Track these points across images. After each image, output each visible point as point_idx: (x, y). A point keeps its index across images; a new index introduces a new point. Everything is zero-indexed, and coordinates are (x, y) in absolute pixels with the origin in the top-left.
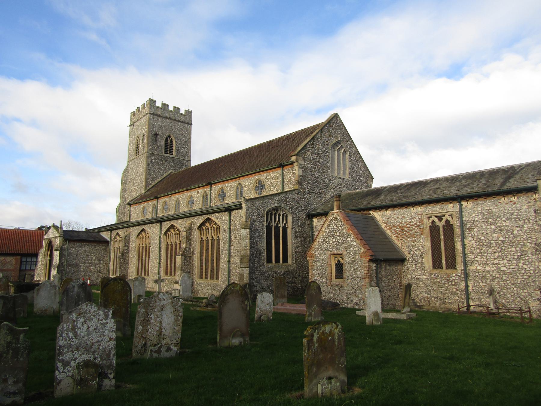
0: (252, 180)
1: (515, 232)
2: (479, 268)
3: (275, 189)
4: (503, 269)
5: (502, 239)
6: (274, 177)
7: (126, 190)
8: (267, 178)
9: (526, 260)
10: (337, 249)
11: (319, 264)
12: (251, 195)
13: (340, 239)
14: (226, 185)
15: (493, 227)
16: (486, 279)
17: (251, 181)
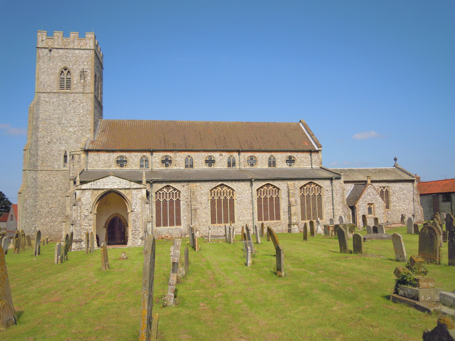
0: (284, 155)
1: (408, 195)
2: (397, 208)
3: (305, 164)
4: (405, 208)
5: (404, 197)
6: (303, 157)
8: (298, 156)
9: (411, 205)
10: (371, 201)
11: (362, 208)
12: (284, 165)
13: (373, 197)
14: (258, 155)
15: (402, 193)
16: (400, 212)
17: (284, 156)
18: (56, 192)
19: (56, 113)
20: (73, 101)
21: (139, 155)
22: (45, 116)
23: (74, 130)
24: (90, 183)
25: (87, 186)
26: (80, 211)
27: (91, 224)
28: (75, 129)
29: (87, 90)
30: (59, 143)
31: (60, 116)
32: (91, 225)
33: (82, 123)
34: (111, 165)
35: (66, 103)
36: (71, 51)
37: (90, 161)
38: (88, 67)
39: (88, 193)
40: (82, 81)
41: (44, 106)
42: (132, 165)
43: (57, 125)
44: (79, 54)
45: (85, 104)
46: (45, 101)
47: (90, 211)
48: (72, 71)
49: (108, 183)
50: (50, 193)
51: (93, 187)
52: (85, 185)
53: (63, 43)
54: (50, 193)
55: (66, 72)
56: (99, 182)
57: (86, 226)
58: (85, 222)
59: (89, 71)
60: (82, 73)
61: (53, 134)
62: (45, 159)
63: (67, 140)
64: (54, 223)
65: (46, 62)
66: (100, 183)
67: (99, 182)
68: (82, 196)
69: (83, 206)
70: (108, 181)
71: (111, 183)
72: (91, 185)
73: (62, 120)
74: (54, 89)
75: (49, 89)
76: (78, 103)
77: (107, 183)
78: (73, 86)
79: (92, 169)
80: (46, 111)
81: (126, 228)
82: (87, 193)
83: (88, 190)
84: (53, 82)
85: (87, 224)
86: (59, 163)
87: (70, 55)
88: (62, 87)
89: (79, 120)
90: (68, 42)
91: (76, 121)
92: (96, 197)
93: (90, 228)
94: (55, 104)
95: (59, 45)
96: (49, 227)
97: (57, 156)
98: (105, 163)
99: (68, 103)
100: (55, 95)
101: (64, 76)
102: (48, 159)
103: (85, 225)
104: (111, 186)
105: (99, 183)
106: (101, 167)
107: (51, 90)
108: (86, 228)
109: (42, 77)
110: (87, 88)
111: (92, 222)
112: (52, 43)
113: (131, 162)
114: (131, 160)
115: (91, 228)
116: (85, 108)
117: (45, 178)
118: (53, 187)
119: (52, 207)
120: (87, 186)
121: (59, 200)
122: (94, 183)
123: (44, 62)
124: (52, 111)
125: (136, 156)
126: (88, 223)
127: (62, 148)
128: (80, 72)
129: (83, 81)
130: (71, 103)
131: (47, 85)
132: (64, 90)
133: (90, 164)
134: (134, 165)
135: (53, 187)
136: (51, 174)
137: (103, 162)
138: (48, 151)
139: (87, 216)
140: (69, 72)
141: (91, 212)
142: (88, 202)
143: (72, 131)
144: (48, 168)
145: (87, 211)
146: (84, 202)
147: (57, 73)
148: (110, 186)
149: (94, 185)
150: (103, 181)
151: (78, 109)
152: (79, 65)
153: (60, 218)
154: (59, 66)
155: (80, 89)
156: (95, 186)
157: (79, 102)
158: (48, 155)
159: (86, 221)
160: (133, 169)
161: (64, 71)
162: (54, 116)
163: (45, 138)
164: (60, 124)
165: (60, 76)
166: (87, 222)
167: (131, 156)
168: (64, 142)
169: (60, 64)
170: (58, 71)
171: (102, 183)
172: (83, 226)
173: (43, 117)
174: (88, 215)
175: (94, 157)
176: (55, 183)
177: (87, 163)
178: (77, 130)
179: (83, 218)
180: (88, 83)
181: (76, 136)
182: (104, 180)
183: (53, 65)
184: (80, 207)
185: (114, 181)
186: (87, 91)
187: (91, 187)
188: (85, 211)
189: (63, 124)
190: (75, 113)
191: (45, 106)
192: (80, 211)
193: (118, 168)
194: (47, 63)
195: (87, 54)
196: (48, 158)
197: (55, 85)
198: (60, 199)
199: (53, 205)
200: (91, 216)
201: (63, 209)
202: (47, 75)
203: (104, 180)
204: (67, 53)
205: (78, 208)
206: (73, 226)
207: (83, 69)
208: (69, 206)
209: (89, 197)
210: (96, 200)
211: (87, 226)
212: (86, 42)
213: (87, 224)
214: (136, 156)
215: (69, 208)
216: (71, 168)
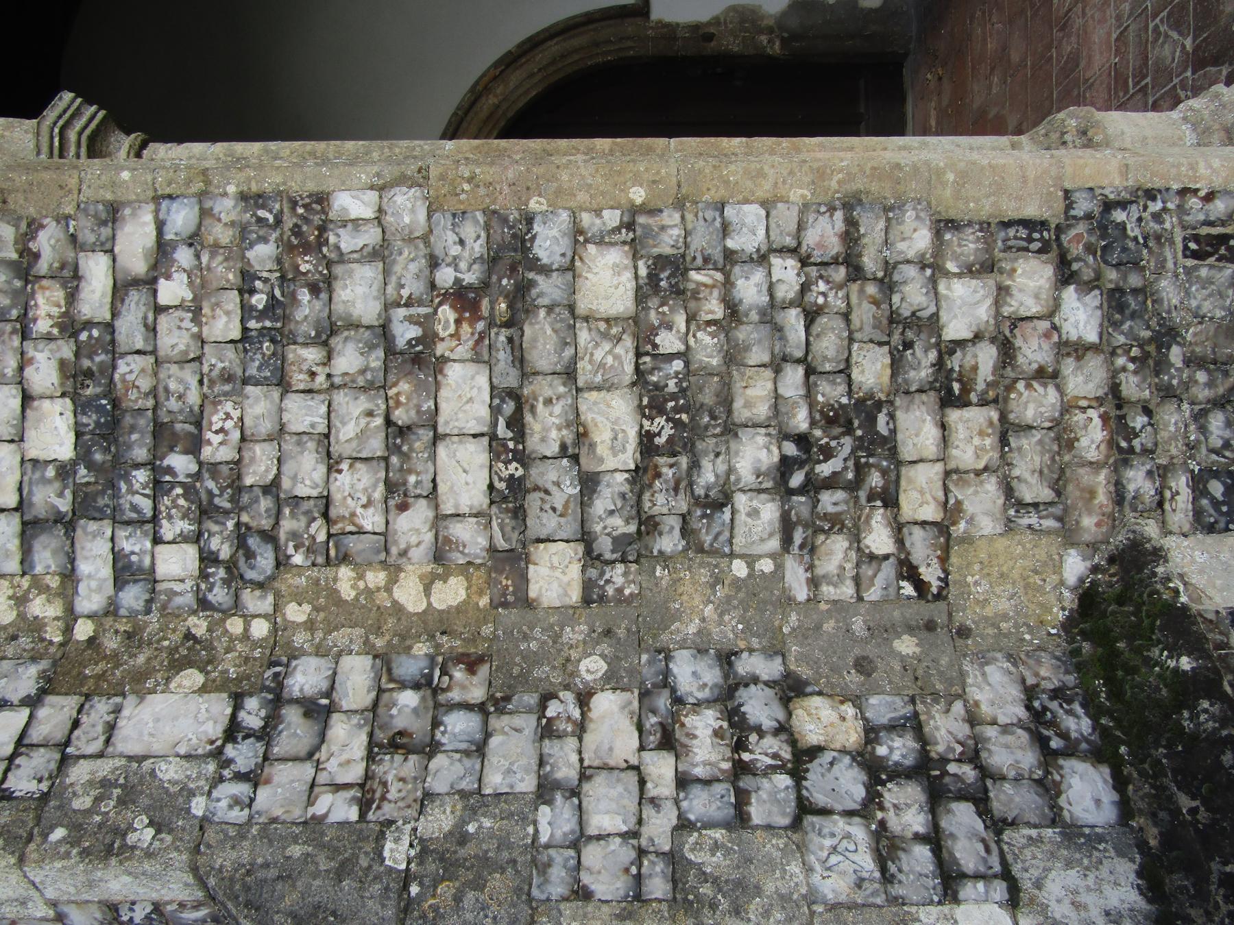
81: (669, 31)
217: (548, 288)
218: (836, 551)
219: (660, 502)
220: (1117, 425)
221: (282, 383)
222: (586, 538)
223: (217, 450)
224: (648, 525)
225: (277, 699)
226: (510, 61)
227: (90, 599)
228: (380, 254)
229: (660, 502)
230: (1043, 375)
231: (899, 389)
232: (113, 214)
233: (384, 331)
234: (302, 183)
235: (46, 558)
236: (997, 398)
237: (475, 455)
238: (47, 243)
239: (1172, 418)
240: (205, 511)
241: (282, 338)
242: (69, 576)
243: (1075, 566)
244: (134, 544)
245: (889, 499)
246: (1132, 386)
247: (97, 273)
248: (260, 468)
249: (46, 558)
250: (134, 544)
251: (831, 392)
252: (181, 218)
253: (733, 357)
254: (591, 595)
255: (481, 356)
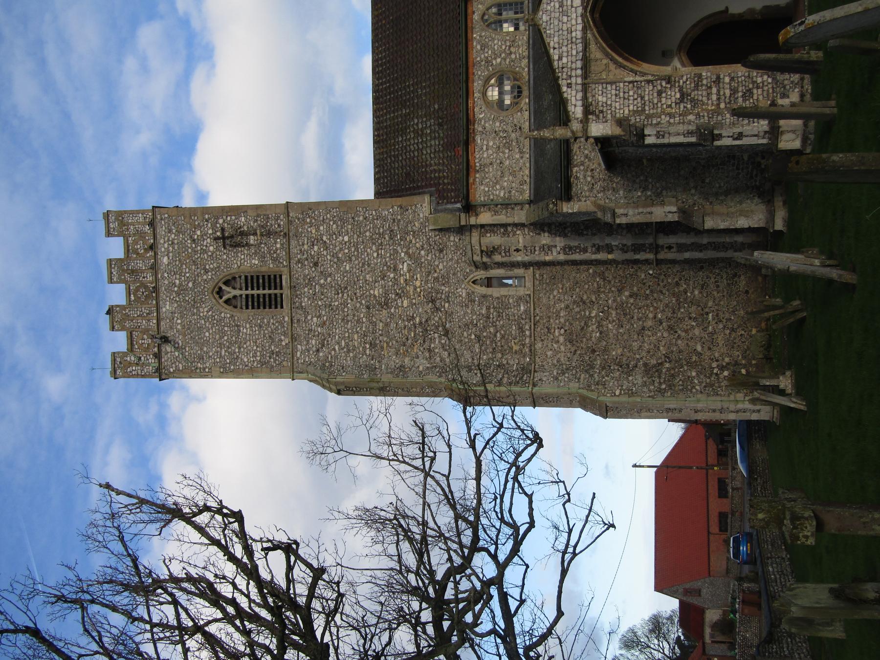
7: (402, 367)
18: (606, 308)
19: (354, 315)
20: (316, 264)
21: (481, 36)
22: (365, 348)
23: (406, 258)
24: (564, 89)
25: (573, 99)
26: (663, 117)
27: (714, 78)
28: (403, 254)
29: (279, 225)
30: (449, 302)
31: (363, 302)
32: (718, 78)
33: (382, 235)
34: (515, 125)
35: (321, 286)
36: (163, 278)
37: (502, 195)
38: (209, 225)
39: (601, 97)
40: (252, 240)
41: (333, 353)
42: (513, 56)
43: (392, 310)
44: (171, 254)
45: (321, 228)
46: (318, 351)
47: (664, 84)
48: (225, 273)
49: (565, 28)
50: (610, 326)
51: (579, 80)
52: (571, 108)
53: (142, 303)
54: (610, 326)
55: (229, 293)
56: (560, 58)
57: (722, 93)
58: (705, 99)
59: (221, 221)
60: (228, 242)
61: (421, 323)
62: (499, 344)
63: (436, 279)
64: (707, 310)
65: (201, 349)
66: (565, 54)
67: (560, 58)
68: (609, 116)
69: (647, 108)
70: (556, 29)
71: (565, 19)
72: (569, 86)
73: (375, 296)
74: (281, 323)
75: (283, 338)
76: (319, 249)
77: (565, 33)
78: (270, 266)
79: (526, 187)
80: (347, 345)
81: (733, 15)
82: (600, 98)
83: (589, 95)
84: (261, 326)
85: (714, 90)
86: (511, 301)
87: (177, 282)
88: (275, 302)
89: (374, 244)
90: (137, 290)
91: (375, 255)
92: (612, 67)
93: (727, 80)
94: (325, 318)
95: (148, 314)
96: (721, 326)
97: (488, 308)
98: (508, 145)
99: (322, 281)
100: (298, 321)
101: (241, 296)
102: (498, 335)
103: (714, 97)
104: (574, 16)
105: (565, 60)
106: (522, 157)
107: (285, 334)
108: (728, 92)
109: (246, 360)
110: (272, 225)
111: (704, 74)
112: (145, 337)
113: (505, 59)
114: (499, 60)
115: (729, 75)
116: (334, 226)
117: (558, 342)
118: (590, 318)
119: (655, 317)
120: (573, 99)
121: (631, 296)
122: (565, 76)
123: (201, 358)
124: (349, 326)
125: (484, 47)
126: (710, 88)
127: (464, 295)
128: (225, 248)
129: (252, 237)
130: (322, 272)
131: (270, 346)
132: (282, 295)
133: (510, 192)
134: (513, 49)
135: (590, 318)
136: (546, 325)
137: (504, 153)
138: (473, 337)
139: (683, 95)
140: (227, 283)
141: (668, 82)
142: (631, 93)
143: (408, 265)
144: (527, 333)
145: (664, 95)
146: (631, 108)
147: (232, 316)
148: (574, 22)
149: (570, 77)
150: (557, 46)
151: (341, 249)
152: (205, 252)
153: (692, 293)
154: (210, 313)
155: (278, 246)
156: (573, 74)
157: (316, 248)
158: (485, 334)
159: (700, 94)
160: (526, 54)
161: (225, 298)
162: (364, 320)
163: (432, 346)
164: (386, 304)
165: (241, 308)
166: (705, 93)
167: (483, 63)
168: (443, 288)
169: (206, 309)
170: (227, 313)
171: (564, 49)
172: (718, 105)
173: (368, 352)
174: (681, 91)
175: (488, 180)
176: (577, 309)
177: (508, 205)
178: (405, 250)
179: (689, 106)
180: (256, 221)
181: (423, 253)
182: (552, 44)
183: (208, 331)
184: (649, 117)
185: (557, 5)
186: (282, 223)
187: (579, 87)
188: (664, 100)
189: (386, 293)
190: (353, 258)
191: (334, 349)
192: (663, 117)
193: (523, 103)
194: (205, 349)
195: (170, 231)
196: (495, 336)
197: (269, 322)
198: (627, 293)
199: (647, 317)
200: (685, 78)
201: (662, 284)
202: (239, 348)
203: (552, 42)
204: (169, 290)
205: (654, 122)
206: (720, 137)
207: (216, 239)
208: (649, 210)
209: (614, 92)
210: (624, 67)
211: (718, 91)
212: (134, 235)
213: (714, 90)
214: (484, 47)
215: (653, 209)
216: (526, 259)
217: (722, 80)
218: (748, 102)
219: (732, 99)
220: (773, 90)
221: (698, 90)
222: (725, 102)
223: (692, 96)
224: (731, 101)
225: (700, 116)
226: (694, 26)
227: (681, 110)
228: (706, 78)
229: (732, 99)
230: (767, 86)
231: (753, 88)
232: (682, 76)
233: (707, 85)
234: (699, 72)
235: (678, 106)
236: (762, 88)
237: (715, 96)
238: (677, 79)
239: (778, 89)
240: (691, 102)
241: (698, 86)
242: (680, 108)
243: (769, 102)
244: (685, 105)
245: (752, 97)
246: (775, 86)
247: (681, 82)
248: (696, 97)
249: (678, 106)
250: (685, 105)
251: (747, 88)
252: (689, 76)
253: (738, 86)
254: (726, 107)
255: (716, 87)
